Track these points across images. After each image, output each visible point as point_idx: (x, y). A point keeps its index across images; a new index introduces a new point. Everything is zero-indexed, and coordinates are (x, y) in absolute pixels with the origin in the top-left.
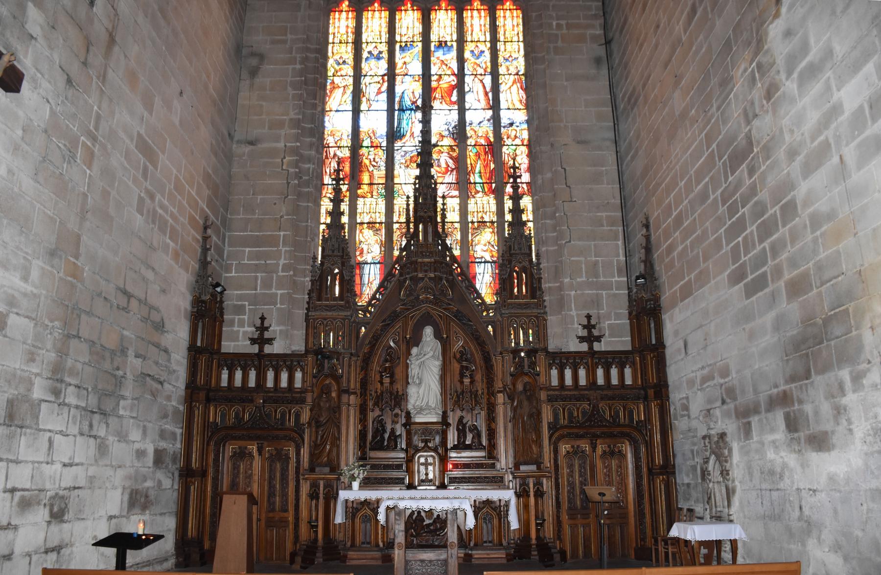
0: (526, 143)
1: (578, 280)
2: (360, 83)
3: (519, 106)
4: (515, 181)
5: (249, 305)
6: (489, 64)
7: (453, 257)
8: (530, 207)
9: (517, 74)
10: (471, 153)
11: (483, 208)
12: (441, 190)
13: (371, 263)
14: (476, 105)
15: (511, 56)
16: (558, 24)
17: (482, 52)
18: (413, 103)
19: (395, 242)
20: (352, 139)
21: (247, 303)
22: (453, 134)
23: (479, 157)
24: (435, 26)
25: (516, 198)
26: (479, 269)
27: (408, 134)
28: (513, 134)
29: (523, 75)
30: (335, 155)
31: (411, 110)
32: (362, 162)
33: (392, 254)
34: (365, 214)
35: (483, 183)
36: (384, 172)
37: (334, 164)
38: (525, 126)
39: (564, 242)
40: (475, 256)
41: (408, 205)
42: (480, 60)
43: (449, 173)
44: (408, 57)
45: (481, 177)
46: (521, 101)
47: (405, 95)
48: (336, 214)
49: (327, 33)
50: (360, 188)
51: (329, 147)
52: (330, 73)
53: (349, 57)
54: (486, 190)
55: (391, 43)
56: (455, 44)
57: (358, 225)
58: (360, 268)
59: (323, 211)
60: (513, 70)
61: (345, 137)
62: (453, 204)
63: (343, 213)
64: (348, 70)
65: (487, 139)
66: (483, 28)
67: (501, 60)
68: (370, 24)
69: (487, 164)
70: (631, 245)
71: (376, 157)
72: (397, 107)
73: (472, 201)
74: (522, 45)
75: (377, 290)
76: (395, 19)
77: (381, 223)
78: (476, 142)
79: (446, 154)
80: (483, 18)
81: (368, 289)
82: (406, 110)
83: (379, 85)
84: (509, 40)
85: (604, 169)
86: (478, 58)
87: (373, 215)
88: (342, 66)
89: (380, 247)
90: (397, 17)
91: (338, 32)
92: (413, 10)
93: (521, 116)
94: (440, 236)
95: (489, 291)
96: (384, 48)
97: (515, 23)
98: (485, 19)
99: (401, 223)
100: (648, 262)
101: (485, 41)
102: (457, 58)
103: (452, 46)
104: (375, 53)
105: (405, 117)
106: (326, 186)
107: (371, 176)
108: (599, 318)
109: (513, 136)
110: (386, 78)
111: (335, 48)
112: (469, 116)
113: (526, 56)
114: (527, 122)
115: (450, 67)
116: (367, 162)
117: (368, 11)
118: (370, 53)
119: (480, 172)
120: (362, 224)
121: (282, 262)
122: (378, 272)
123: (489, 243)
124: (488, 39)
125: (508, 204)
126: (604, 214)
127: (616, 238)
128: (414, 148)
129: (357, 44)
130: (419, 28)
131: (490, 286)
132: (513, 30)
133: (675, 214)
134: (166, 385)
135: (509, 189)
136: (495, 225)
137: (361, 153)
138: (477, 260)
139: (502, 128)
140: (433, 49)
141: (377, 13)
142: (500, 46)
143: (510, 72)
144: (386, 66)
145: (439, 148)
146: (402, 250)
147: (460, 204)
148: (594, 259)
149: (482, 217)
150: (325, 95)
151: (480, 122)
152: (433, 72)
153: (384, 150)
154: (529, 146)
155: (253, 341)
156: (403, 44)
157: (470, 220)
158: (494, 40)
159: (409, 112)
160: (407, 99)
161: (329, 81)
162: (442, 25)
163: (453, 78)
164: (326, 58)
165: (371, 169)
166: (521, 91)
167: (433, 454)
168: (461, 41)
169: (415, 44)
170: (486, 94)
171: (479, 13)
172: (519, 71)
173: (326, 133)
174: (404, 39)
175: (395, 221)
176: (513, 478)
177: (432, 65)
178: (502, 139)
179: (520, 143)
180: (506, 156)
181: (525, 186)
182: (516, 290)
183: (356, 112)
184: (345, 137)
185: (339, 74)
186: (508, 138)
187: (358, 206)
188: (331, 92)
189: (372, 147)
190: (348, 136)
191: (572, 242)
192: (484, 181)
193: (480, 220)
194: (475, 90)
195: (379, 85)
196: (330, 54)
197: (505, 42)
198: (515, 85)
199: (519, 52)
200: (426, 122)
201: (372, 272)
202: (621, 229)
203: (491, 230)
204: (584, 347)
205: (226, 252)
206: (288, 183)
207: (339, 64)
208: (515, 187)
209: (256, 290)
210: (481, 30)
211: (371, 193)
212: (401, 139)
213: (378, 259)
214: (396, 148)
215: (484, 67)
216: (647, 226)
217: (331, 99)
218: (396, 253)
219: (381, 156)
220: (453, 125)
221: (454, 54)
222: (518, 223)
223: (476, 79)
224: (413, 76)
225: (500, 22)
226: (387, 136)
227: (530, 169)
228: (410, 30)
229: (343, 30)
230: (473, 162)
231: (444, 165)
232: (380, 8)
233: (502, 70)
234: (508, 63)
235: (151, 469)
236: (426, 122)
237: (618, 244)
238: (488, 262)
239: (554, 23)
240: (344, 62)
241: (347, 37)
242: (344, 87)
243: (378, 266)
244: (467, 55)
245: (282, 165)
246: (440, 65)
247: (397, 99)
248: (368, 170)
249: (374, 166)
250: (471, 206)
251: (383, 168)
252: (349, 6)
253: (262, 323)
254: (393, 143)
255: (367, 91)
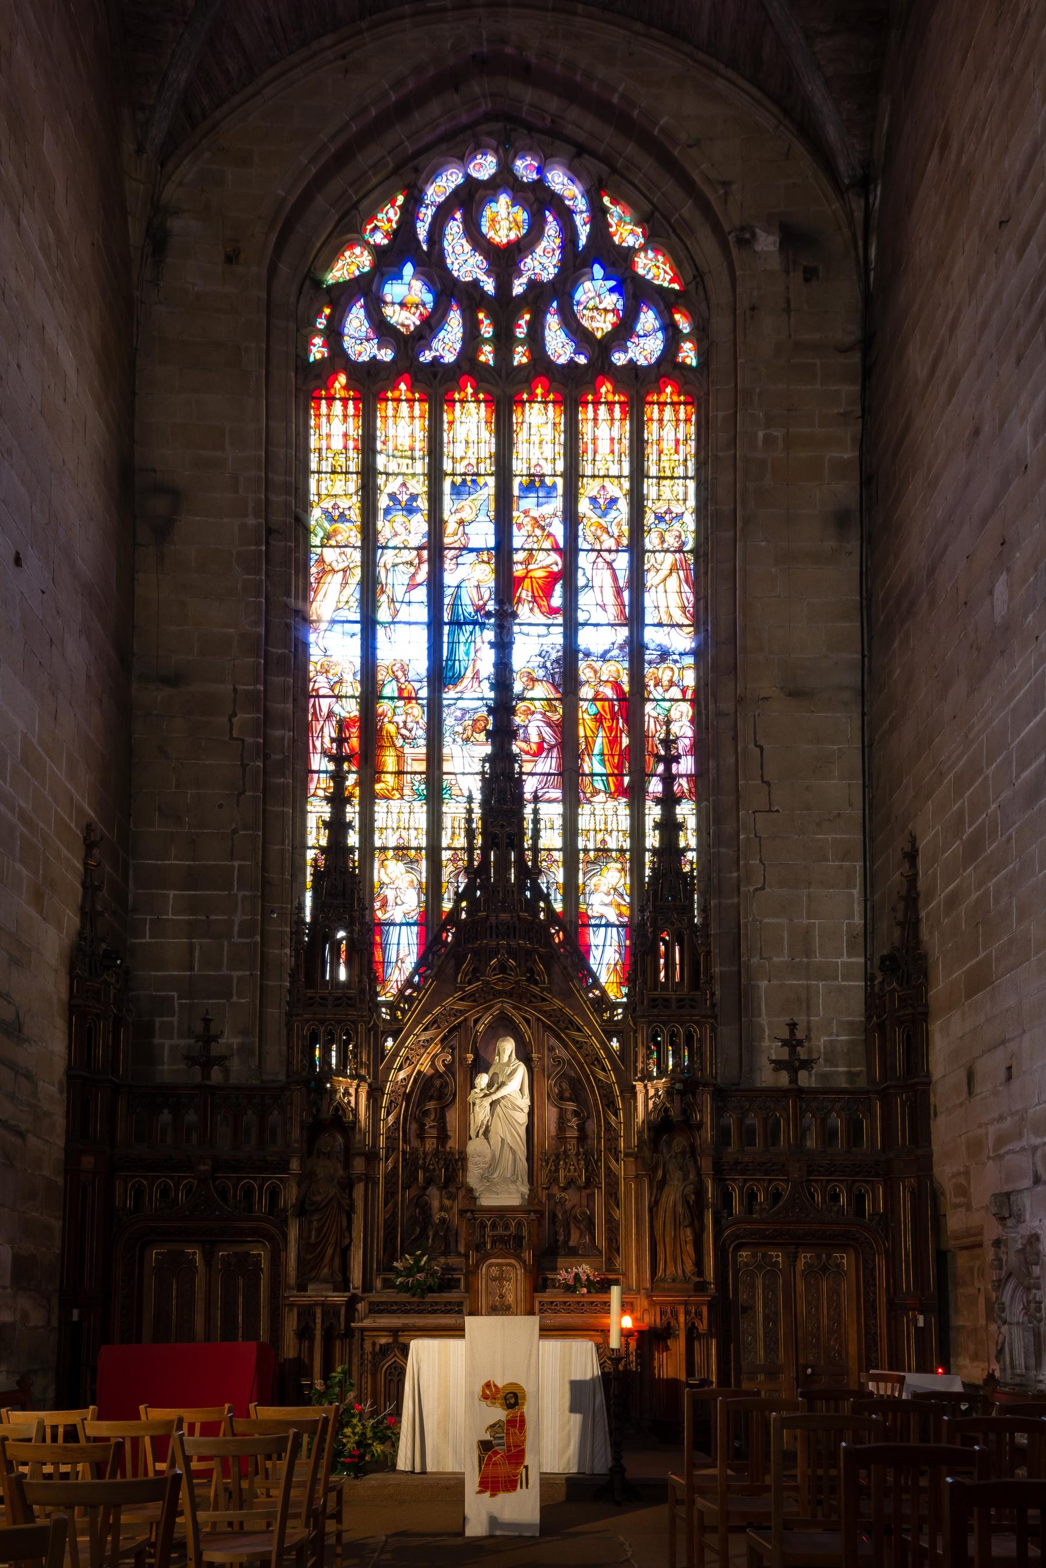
0: (689, 695)
1: (775, 959)
2: (375, 565)
3: (679, 618)
4: (668, 768)
5: (179, 999)
6: (625, 529)
7: (549, 910)
8: (691, 822)
9: (679, 550)
10: (586, 716)
11: (606, 823)
12: (530, 785)
13: (401, 925)
14: (599, 617)
15: (669, 511)
16: (767, 437)
17: (613, 501)
18: (478, 609)
19: (445, 885)
20: (361, 682)
21: (175, 994)
22: (552, 675)
23: (601, 723)
24: (521, 437)
25: (669, 801)
26: (596, 938)
27: (469, 674)
28: (666, 676)
29: (691, 551)
30: (331, 714)
31: (475, 623)
32: (381, 728)
33: (440, 907)
34: (390, 831)
35: (607, 775)
36: (424, 750)
37: (330, 731)
38: (689, 660)
39: (752, 889)
40: (590, 913)
41: (470, 811)
42: (609, 518)
43: (544, 755)
44: (467, 508)
45: (603, 763)
46: (684, 608)
47: (463, 592)
48: (337, 826)
49: (307, 450)
50: (379, 781)
51: (318, 696)
52: (315, 541)
53: (352, 505)
54: (613, 789)
55: (435, 475)
56: (560, 482)
57: (377, 853)
58: (381, 934)
59: (312, 821)
60: (671, 541)
61: (348, 677)
62: (552, 812)
63: (350, 825)
64: (350, 533)
65: (617, 686)
66: (616, 447)
67: (649, 519)
68: (391, 432)
69: (616, 736)
70: (877, 896)
71: (409, 720)
72: (446, 618)
73: (585, 810)
74: (691, 485)
75: (416, 971)
76: (442, 422)
77: (418, 849)
78: (597, 693)
79: (539, 717)
80: (617, 424)
81: (397, 971)
82: (466, 623)
83: (412, 570)
84: (668, 473)
85: (836, 747)
86: (604, 514)
87: (404, 834)
88: (339, 525)
89: (418, 895)
90: (446, 418)
91: (328, 448)
92: (478, 401)
93: (682, 641)
94: (531, 873)
95: (613, 978)
96: (419, 486)
97: (681, 436)
98: (622, 426)
99: (455, 849)
100: (911, 925)
101: (620, 477)
102: (564, 512)
103: (554, 486)
104: (404, 498)
105: (462, 639)
106: (316, 776)
107: (400, 758)
108: (809, 1029)
109: (666, 683)
110: (425, 554)
111: (323, 484)
112: (586, 638)
113: (700, 512)
114: (695, 653)
115: (549, 535)
116: (391, 728)
117: (386, 400)
118: (392, 496)
119: (602, 754)
120: (384, 849)
121: (238, 919)
122: (414, 940)
123: (615, 889)
124: (626, 472)
125: (653, 813)
126: (829, 837)
127: (849, 884)
128: (480, 703)
129: (368, 475)
130: (488, 446)
131: (615, 969)
132: (677, 452)
133: (969, 831)
134: (32, 1140)
135: (655, 786)
136: (628, 855)
137: (380, 711)
138: (593, 922)
139: (646, 665)
140: (516, 492)
141: (404, 406)
142: (650, 488)
143: (665, 546)
144: (425, 527)
145: (527, 703)
146: (459, 897)
147: (564, 816)
148: (805, 921)
149: (604, 841)
150: (307, 585)
151: (606, 652)
152: (517, 543)
153: (422, 706)
154: (694, 702)
155: (190, 1060)
156: (458, 480)
157: (581, 846)
158: (638, 474)
159: (470, 628)
160: (466, 600)
161: (314, 557)
162: (535, 439)
163: (555, 557)
164: (305, 506)
165: (399, 742)
166: (686, 588)
167: (513, 1261)
168: (572, 476)
169: (481, 481)
170: (618, 592)
171: (611, 411)
172: (684, 544)
173: (311, 668)
174: (460, 468)
175: (444, 845)
176: (650, 1305)
177: (515, 527)
178: (644, 686)
179: (679, 696)
180: (652, 720)
181: (683, 782)
182: (662, 974)
183: (369, 625)
184: (348, 677)
185: (333, 542)
186: (655, 686)
187: (376, 816)
188: (319, 581)
189: (400, 697)
190: (355, 674)
191: (767, 889)
192: (609, 771)
193: (599, 846)
194: (597, 583)
195: (412, 570)
196: (313, 498)
197: (659, 478)
198: (674, 575)
199: (685, 500)
200: (503, 646)
201: (404, 941)
202: (859, 865)
203: (619, 866)
204: (783, 1079)
205: (130, 897)
206: (244, 766)
207: (332, 520)
208: (668, 779)
209: (192, 969)
210: (612, 452)
211: (400, 789)
212: (455, 685)
213: (414, 916)
214: (445, 702)
215: (616, 534)
216: (911, 856)
217: (319, 597)
218: (447, 906)
219: (418, 713)
220: (554, 656)
221: (557, 504)
222: (670, 851)
223: (600, 560)
224: (478, 551)
225: (651, 432)
226: (428, 677)
227: (698, 748)
228: (473, 449)
229: (337, 444)
230: (589, 733)
231: (534, 738)
232: (410, 396)
233: (651, 541)
234: (663, 526)
235: (9, 1290)
236: (503, 646)
237: (853, 894)
238: (613, 925)
239: (761, 434)
240: (342, 515)
241: (347, 459)
242: (344, 571)
243: (415, 929)
244: (584, 506)
245: (231, 730)
246: (529, 528)
247: (447, 601)
248: (394, 746)
249: (404, 737)
250: (584, 822)
251: (422, 742)
252: (345, 388)
253: (207, 1028)
254: (440, 692)
255: (390, 581)
